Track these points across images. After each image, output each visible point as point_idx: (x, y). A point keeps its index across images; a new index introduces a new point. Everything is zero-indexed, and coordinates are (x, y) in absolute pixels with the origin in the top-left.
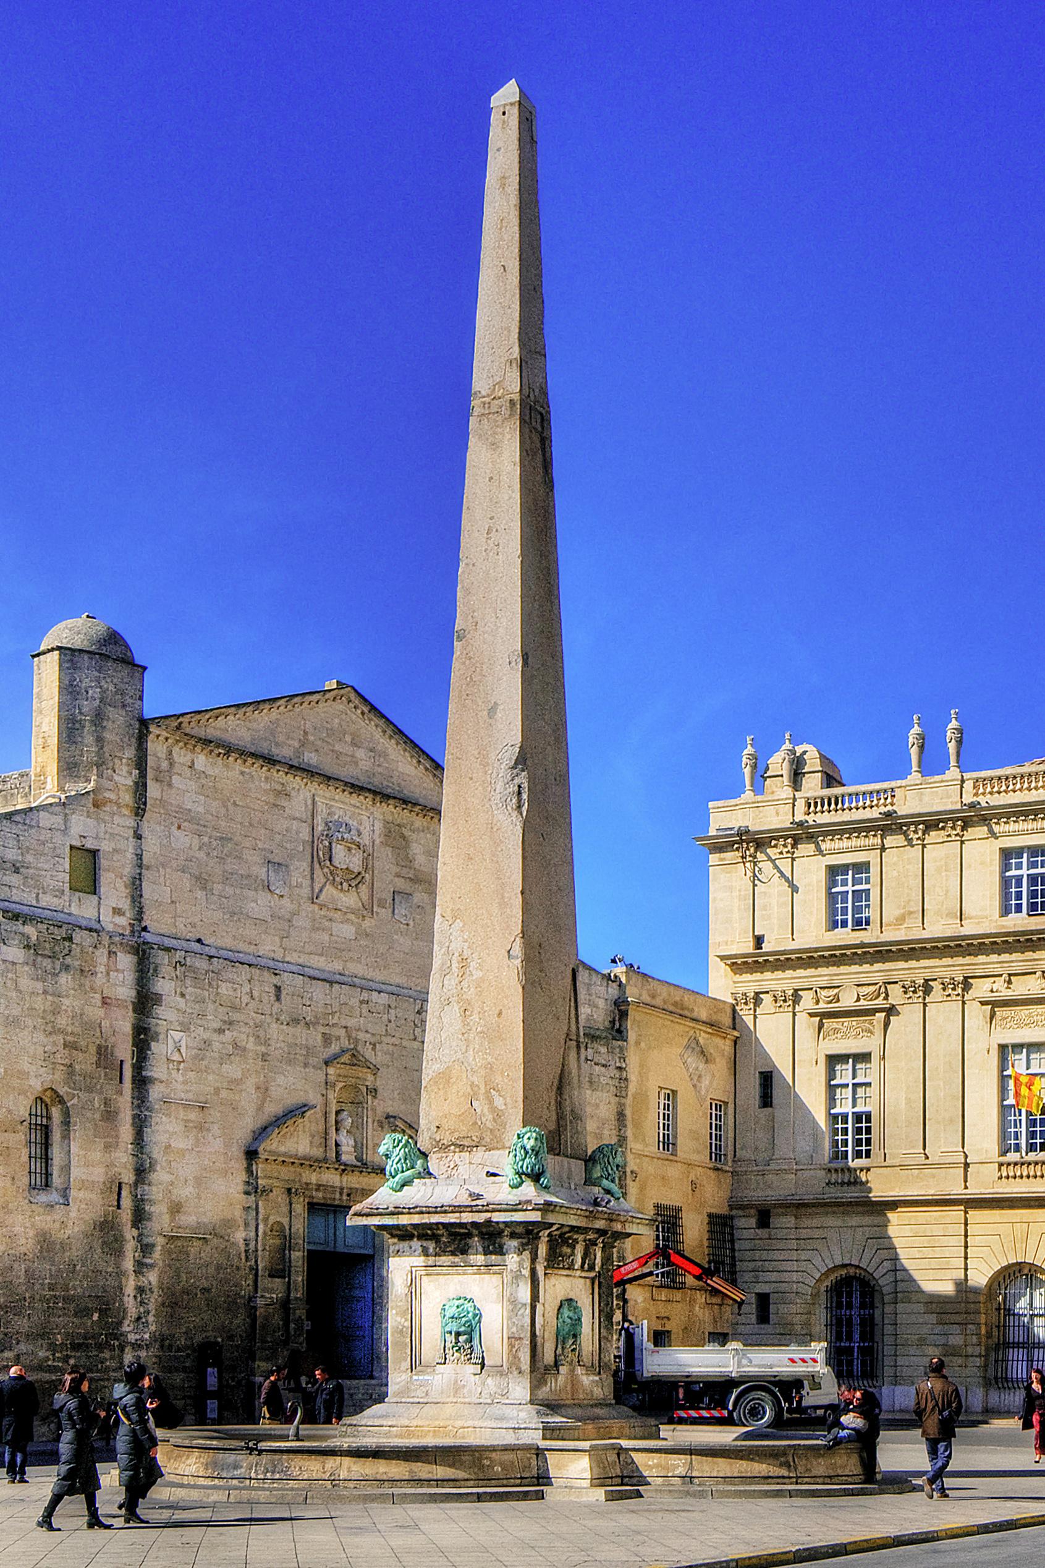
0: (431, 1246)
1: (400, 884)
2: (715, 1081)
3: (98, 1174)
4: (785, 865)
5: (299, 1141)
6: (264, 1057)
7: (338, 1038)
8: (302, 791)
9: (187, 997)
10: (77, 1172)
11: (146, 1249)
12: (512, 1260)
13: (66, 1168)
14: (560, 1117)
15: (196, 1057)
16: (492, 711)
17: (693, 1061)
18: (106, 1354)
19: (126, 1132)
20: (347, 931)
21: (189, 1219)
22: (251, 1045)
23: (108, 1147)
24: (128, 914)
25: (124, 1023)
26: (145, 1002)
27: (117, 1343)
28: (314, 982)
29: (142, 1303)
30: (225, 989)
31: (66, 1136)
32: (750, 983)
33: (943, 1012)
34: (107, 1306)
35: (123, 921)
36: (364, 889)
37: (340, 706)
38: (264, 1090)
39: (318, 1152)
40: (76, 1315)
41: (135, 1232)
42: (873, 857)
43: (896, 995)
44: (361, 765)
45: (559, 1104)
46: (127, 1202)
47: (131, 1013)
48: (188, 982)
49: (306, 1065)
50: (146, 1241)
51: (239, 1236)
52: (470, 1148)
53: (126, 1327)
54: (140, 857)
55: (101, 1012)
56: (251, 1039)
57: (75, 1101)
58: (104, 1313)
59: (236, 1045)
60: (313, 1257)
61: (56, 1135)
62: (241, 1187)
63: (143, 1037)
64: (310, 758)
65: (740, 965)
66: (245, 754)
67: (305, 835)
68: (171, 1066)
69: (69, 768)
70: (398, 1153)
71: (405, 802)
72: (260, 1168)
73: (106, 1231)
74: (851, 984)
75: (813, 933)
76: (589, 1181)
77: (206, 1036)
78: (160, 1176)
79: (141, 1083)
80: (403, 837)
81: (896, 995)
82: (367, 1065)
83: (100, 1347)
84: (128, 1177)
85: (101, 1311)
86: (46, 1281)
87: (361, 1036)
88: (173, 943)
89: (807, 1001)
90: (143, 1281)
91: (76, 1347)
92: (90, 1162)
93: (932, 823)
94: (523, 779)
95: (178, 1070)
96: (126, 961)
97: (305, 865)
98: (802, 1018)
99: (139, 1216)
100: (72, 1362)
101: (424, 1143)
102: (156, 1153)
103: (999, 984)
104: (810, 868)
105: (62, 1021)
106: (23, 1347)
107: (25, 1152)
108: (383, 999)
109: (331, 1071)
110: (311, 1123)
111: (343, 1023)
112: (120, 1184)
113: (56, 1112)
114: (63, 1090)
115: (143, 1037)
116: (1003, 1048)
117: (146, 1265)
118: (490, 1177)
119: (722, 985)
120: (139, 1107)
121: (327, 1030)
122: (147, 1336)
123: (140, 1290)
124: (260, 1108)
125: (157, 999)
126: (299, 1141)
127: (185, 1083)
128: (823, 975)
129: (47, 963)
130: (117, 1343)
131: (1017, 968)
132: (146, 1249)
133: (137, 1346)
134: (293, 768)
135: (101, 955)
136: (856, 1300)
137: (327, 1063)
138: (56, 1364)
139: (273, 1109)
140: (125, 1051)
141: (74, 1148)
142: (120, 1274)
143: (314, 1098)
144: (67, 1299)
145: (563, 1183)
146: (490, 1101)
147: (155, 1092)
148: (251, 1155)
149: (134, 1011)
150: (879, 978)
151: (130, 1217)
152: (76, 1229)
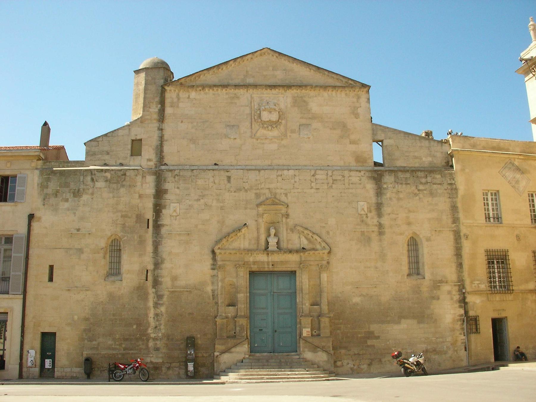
1: (304, 121)
3: (136, 267)
6: (222, 208)
7: (265, 194)
9: (181, 188)
11: (159, 297)
18: (140, 343)
19: (150, 248)
20: (274, 147)
21: (182, 282)
22: (215, 204)
23: (140, 255)
24: (154, 160)
25: (149, 204)
26: (160, 193)
27: (145, 338)
28: (250, 172)
29: (157, 320)
30: (200, 182)
34: (140, 323)
35: (152, 164)
36: (282, 128)
38: (222, 223)
41: (154, 290)
44: (279, 76)
46: (150, 278)
47: (152, 199)
48: (181, 182)
49: (246, 208)
50: (159, 293)
51: (209, 289)
53: (150, 331)
55: (139, 201)
56: (215, 202)
57: (126, 238)
58: (139, 325)
59: (206, 205)
62: (209, 267)
63: (158, 209)
68: (172, 218)
71: (300, 86)
73: (140, 291)
77: (190, 203)
78: (167, 265)
79: (157, 227)
80: (304, 101)
82: (281, 203)
83: (137, 339)
84: (151, 267)
85: (137, 324)
87: (278, 191)
88: (175, 168)
90: (158, 311)
91: (126, 340)
92: (133, 264)
95: (176, 219)
96: (151, 179)
97: (248, 124)
99: (156, 283)
100: (123, 346)
102: (165, 255)
105: (121, 207)
106: (101, 340)
108: (291, 172)
109: (261, 209)
111: (267, 187)
112: (147, 271)
115: (158, 209)
117: (159, 304)
121: (258, 191)
122: (160, 335)
123: (157, 315)
125: (166, 191)
126: (243, 241)
129: (114, 186)
130: (145, 338)
132: (159, 297)
133: (155, 339)
135: (139, 178)
137: (258, 205)
140: (150, 215)
142: (147, 308)
148: (213, 252)
149: (154, 198)
151: (151, 284)
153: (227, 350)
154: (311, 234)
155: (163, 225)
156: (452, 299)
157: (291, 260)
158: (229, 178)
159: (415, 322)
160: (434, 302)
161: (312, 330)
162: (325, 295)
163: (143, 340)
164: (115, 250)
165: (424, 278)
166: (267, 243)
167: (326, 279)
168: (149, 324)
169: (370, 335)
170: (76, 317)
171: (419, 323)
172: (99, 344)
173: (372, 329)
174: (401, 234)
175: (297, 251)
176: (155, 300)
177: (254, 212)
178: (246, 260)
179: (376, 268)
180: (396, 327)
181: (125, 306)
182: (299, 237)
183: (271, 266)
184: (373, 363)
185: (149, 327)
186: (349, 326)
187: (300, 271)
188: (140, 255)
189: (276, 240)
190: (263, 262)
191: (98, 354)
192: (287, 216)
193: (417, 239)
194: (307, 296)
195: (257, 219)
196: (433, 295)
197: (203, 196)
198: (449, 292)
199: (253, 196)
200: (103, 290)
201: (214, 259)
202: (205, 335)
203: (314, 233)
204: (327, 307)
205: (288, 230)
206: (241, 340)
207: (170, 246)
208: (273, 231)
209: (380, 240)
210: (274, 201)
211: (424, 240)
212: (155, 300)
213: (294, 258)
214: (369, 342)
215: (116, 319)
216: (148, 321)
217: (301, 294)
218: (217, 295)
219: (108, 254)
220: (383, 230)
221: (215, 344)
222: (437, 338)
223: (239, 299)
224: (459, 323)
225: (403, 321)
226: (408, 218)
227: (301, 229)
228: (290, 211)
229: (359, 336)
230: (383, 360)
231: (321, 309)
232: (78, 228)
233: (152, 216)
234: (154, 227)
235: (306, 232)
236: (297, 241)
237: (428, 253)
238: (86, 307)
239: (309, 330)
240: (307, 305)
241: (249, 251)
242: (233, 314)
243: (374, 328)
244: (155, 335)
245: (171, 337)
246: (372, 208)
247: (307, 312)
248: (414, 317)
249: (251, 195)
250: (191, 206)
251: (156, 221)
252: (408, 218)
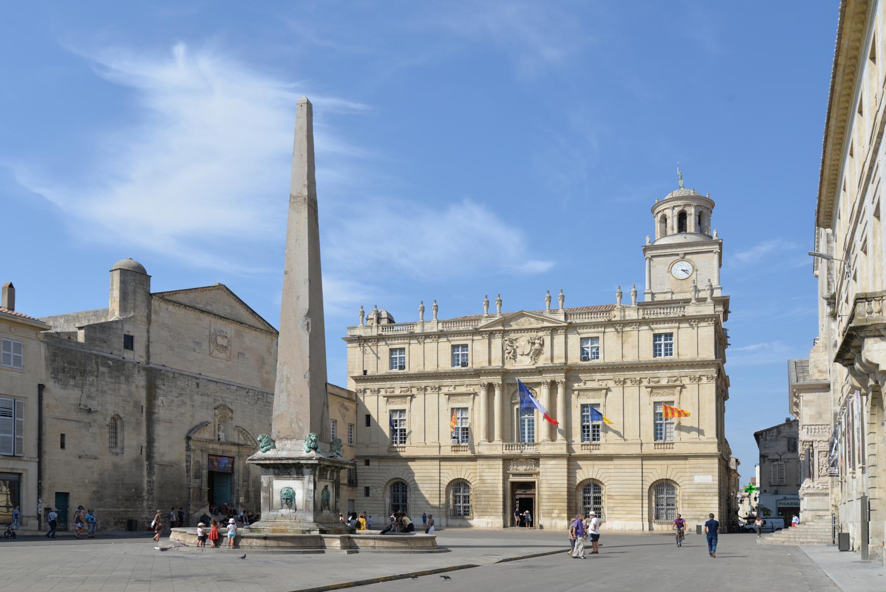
0: (276, 471)
2: (351, 417)
4: (374, 348)
5: (206, 434)
6: (193, 406)
8: (206, 319)
10: (126, 443)
12: (307, 477)
13: (123, 441)
14: (322, 430)
16: (298, 298)
17: (343, 410)
19: (144, 430)
22: (188, 402)
25: (143, 394)
30: (179, 383)
31: (123, 430)
32: (362, 386)
33: (432, 397)
37: (219, 291)
38: (193, 416)
39: (212, 438)
42: (406, 346)
43: (414, 391)
45: (321, 426)
52: (291, 439)
54: (149, 338)
60: (211, 474)
61: (119, 430)
64: (209, 308)
65: (357, 379)
66: (186, 306)
67: (208, 333)
69: (123, 308)
70: (264, 440)
72: (191, 443)
74: (398, 387)
75: (384, 368)
76: (331, 451)
81: (414, 391)
89: (383, 392)
93: (427, 336)
94: (309, 320)
98: (381, 398)
101: (273, 437)
103: (451, 389)
104: (383, 349)
107: (108, 436)
108: (235, 388)
113: (118, 422)
114: (122, 415)
116: (453, 409)
118: (300, 449)
119: (352, 386)
125: (156, 387)
128: (388, 384)
131: (457, 383)
134: (202, 311)
136: (400, 489)
139: (196, 423)
140: (144, 403)
141: (126, 434)
143: (211, 420)
145: (323, 451)
146: (298, 424)
150: (408, 385)
158: (198, 385)
164: (115, 425)
177: (212, 413)
190: (217, 450)
197: (180, 395)
199: (212, 400)
200: (108, 460)
201: (187, 443)
207: (160, 430)
208: (222, 428)
210: (224, 407)
213: (234, 449)
236: (237, 437)
241: (211, 441)
249: (211, 400)
250: (173, 401)
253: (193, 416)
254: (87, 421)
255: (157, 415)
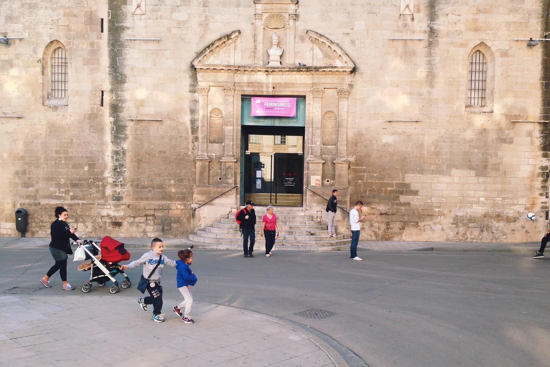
3: (87, 87)
11: (119, 130)
15: (154, 10)
19: (105, 60)
23: (92, 71)
27: (100, 183)
29: (117, 160)
38: (205, 25)
40: (73, 167)
41: (112, 119)
58: (92, 166)
62: (188, 88)
85: (89, 165)
86: (54, 149)
91: (74, 186)
95: (141, 20)
99: (115, 109)
100: (71, 194)
102: (127, 71)
110: (244, 43)
112: (103, 92)
117: (119, 138)
120: (113, 45)
123: (116, 153)
124: (202, 38)
127: (146, 27)
138: (60, 195)
144: (68, 159)
147: (125, 36)
148: (193, 68)
152: (73, 119)
153: (209, 202)
154: (328, 44)
155: (123, 29)
156: (532, 143)
157: (300, 82)
159: (473, 173)
160: (505, 145)
161: (323, 178)
162: (343, 131)
163: (98, 186)
165: (492, 112)
166: (269, 56)
167: (346, 109)
168: (106, 165)
169: (405, 189)
170: (6, 155)
171: (477, 175)
172: (37, 190)
173: (407, 181)
174: (462, 45)
175: (308, 69)
176: (113, 132)
177: (251, 11)
178: (236, 81)
179: (420, 94)
180: (445, 179)
181: (72, 140)
182: (312, 49)
183: (271, 89)
184: (406, 228)
185: (106, 168)
186: (375, 175)
187: (311, 97)
188: (92, 71)
189: (279, 52)
190: (260, 84)
191: (36, 205)
192: (296, 17)
193: (485, 54)
194: (319, 132)
195: (254, 21)
196: (504, 137)
198: (530, 134)
200: (40, 119)
202: (181, 180)
203: (332, 42)
204: (345, 148)
205: (297, 38)
206: (227, 189)
209: (430, 54)
211: (497, 55)
212: (113, 132)
214: (403, 199)
215: (60, 158)
216: (104, 161)
217: (311, 129)
218: (198, 127)
219: (49, 69)
220: (435, 39)
221: (193, 193)
222: (504, 199)
223: (227, 134)
224: (541, 179)
225: (454, 171)
226: (475, 20)
227: (315, 36)
228: (300, 11)
229: (389, 189)
230: (421, 224)
231: (337, 149)
232: (4, 31)
233: (106, 14)
234: (110, 30)
235: (321, 40)
237: (502, 74)
238: (19, 142)
239: (320, 178)
240: (318, 143)
242: (218, 154)
243: (411, 179)
244: (114, 180)
245: (136, 183)
246: (422, 7)
247: (318, 153)
248: (470, 168)
251: (112, 22)
252: (475, 20)
253: (205, 25)
254: (7, 58)
255: (129, 32)
